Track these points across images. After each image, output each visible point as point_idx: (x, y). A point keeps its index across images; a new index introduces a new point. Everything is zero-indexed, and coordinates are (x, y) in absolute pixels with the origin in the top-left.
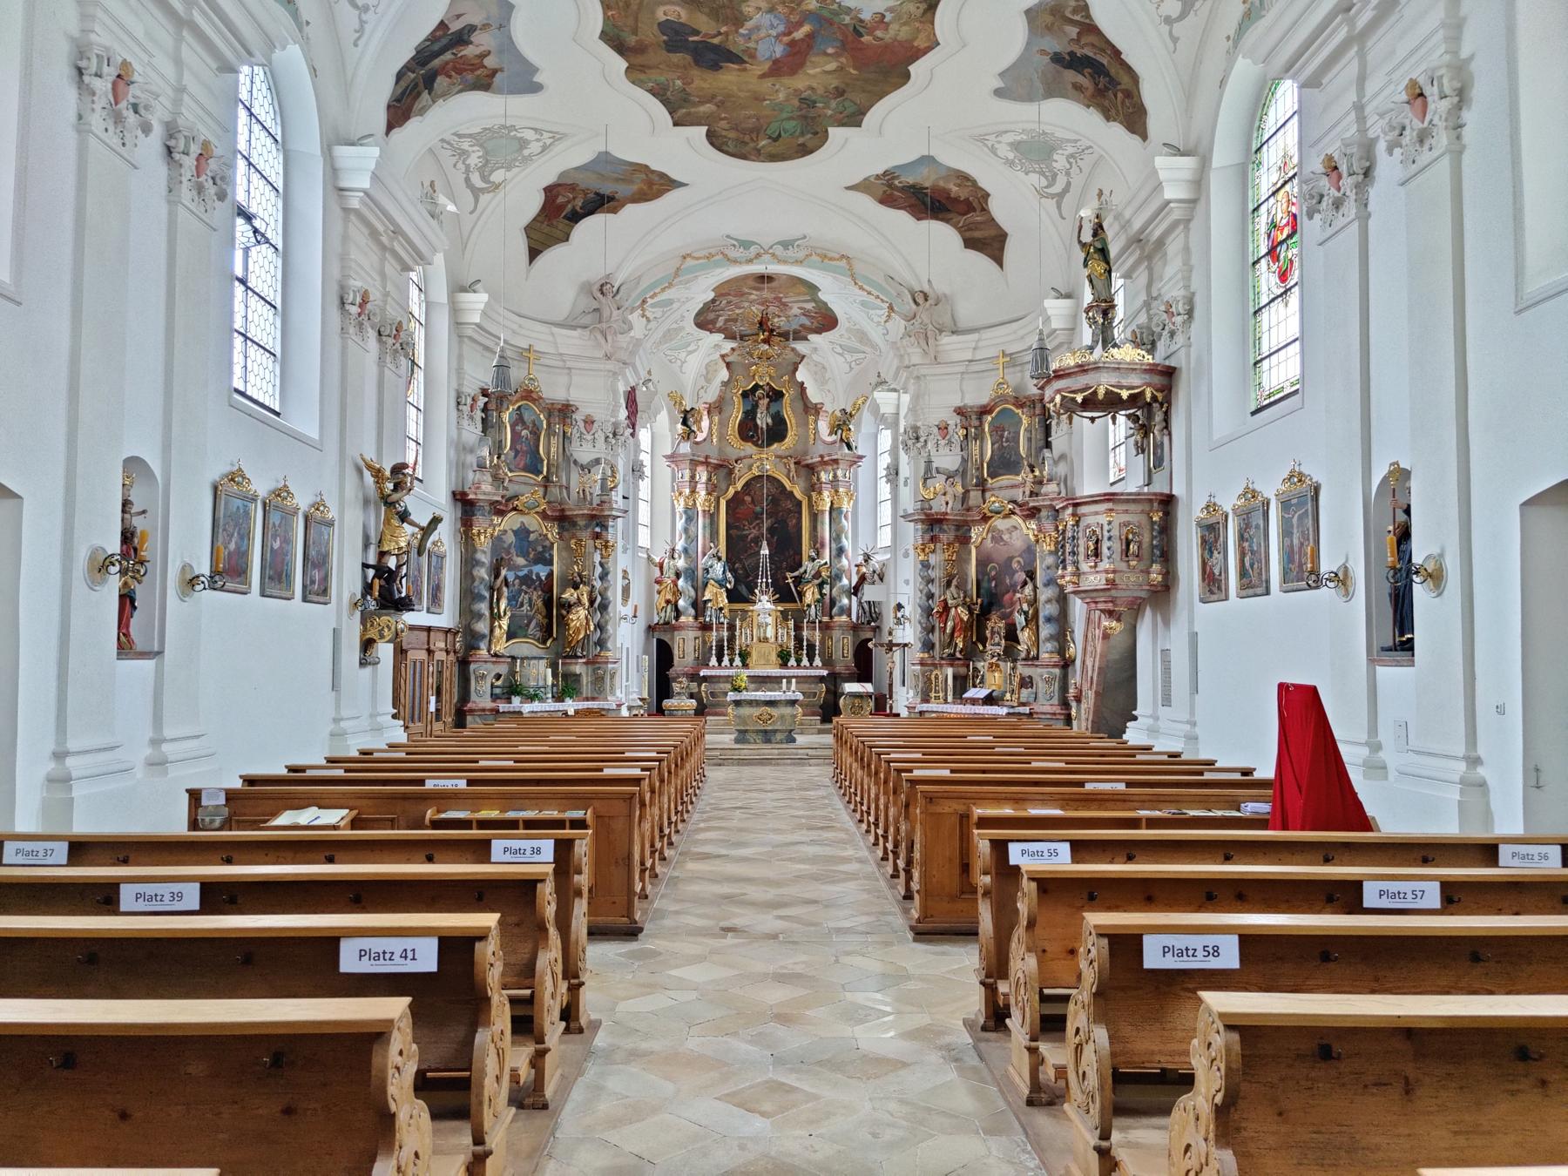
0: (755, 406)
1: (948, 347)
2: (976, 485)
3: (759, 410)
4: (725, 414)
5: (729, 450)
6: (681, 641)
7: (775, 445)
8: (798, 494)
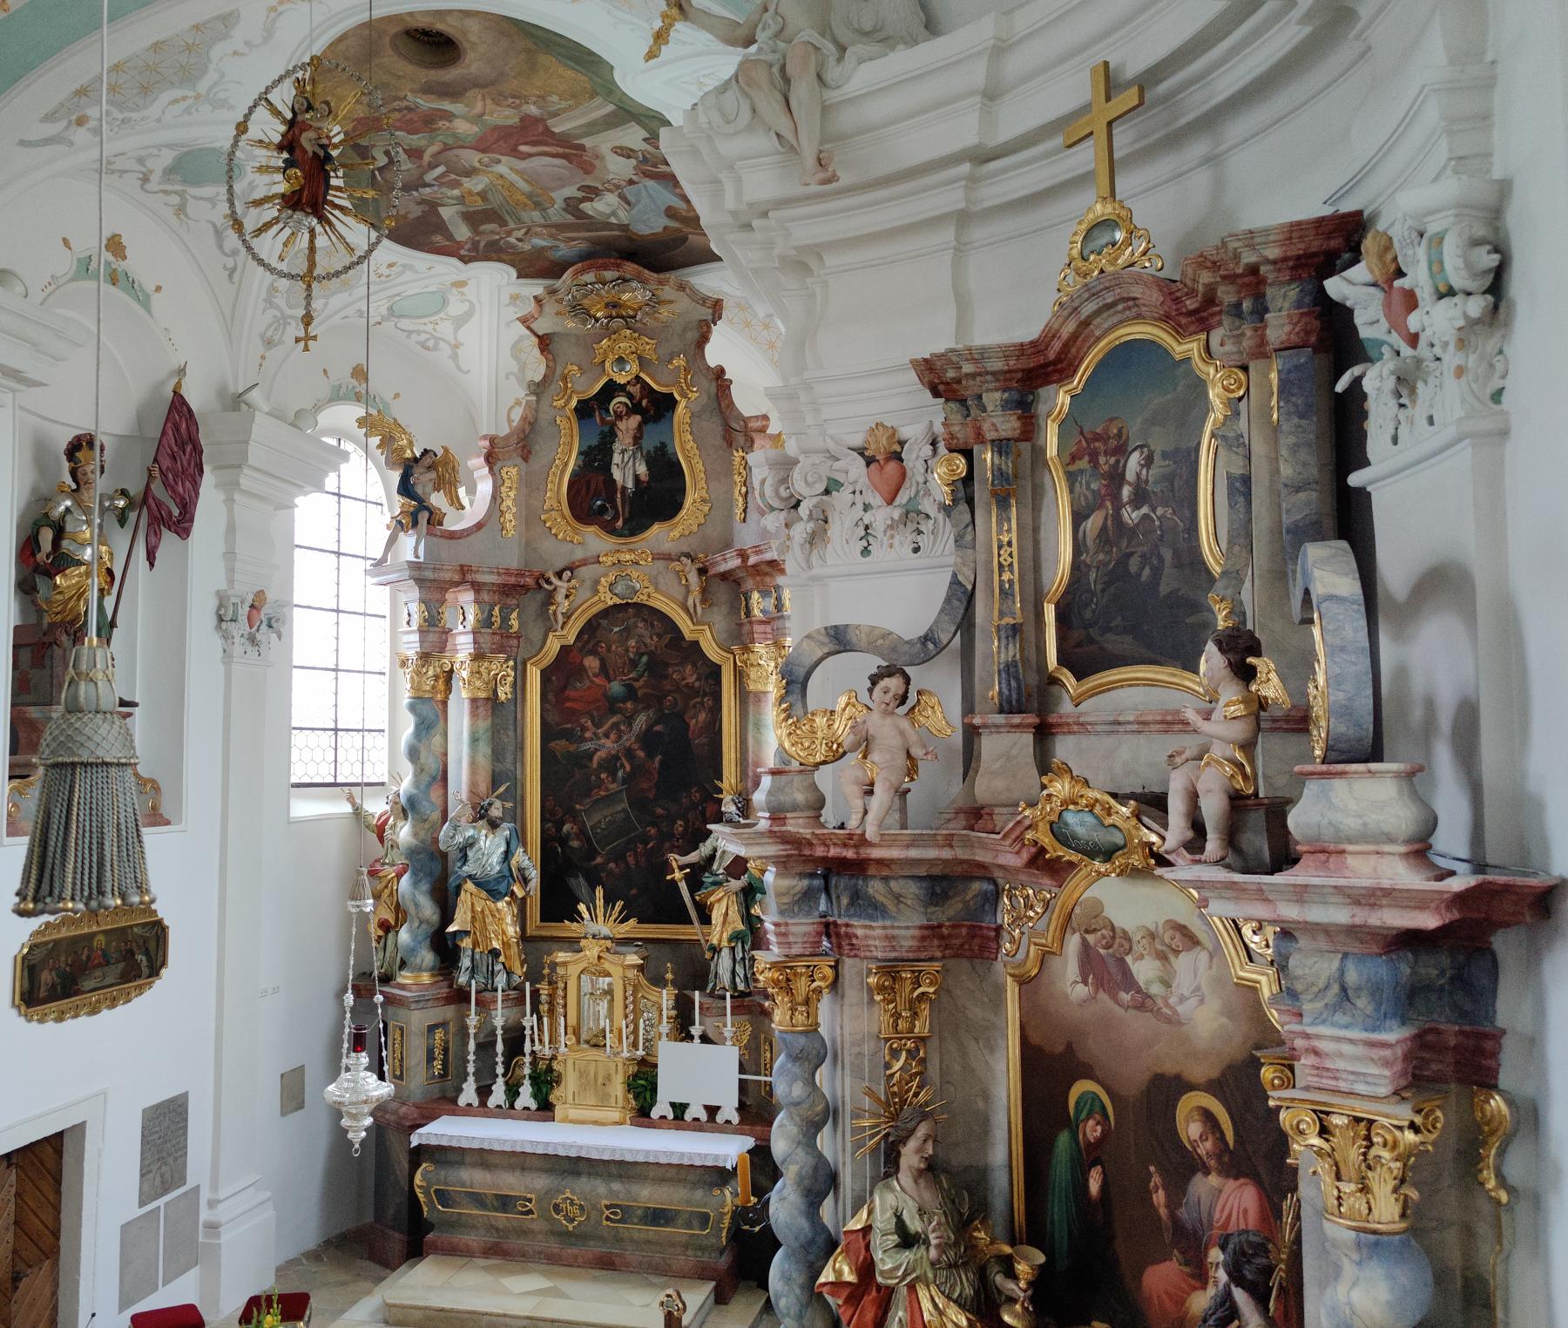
0: (609, 436)
1: (876, 110)
2: (1006, 707)
3: (617, 447)
4: (538, 462)
5: (547, 546)
6: (398, 1036)
7: (656, 528)
8: (712, 651)
